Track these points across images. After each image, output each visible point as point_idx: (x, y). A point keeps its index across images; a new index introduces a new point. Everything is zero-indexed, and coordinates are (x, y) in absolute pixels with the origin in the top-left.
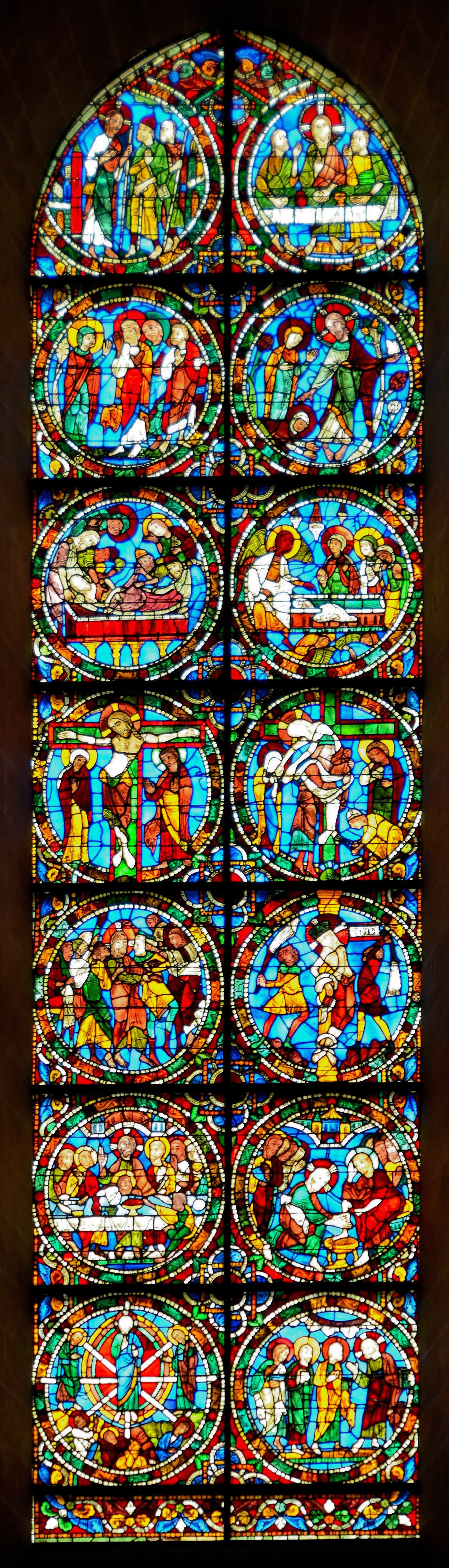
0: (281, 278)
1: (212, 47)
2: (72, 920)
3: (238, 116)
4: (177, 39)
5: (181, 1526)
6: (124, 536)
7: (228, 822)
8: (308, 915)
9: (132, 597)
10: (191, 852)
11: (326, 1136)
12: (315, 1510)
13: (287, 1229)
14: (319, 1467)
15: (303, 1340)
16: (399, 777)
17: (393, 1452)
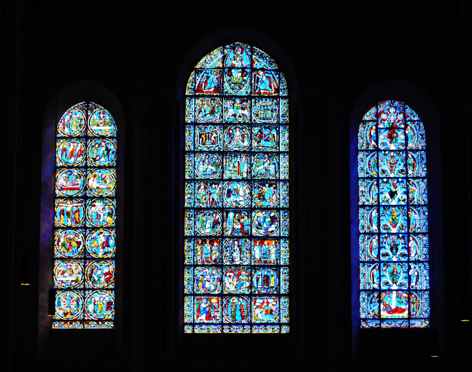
0: (95, 137)
1: (85, 103)
2: (61, 232)
3: (89, 114)
4: (80, 102)
5: (77, 326)
6: (70, 175)
7: (86, 218)
8: (98, 232)
9: (71, 184)
10: (80, 222)
11: (100, 266)
12: (98, 323)
13: (94, 280)
14: (99, 317)
15: (96, 297)
16: (113, 211)
17: (110, 314)
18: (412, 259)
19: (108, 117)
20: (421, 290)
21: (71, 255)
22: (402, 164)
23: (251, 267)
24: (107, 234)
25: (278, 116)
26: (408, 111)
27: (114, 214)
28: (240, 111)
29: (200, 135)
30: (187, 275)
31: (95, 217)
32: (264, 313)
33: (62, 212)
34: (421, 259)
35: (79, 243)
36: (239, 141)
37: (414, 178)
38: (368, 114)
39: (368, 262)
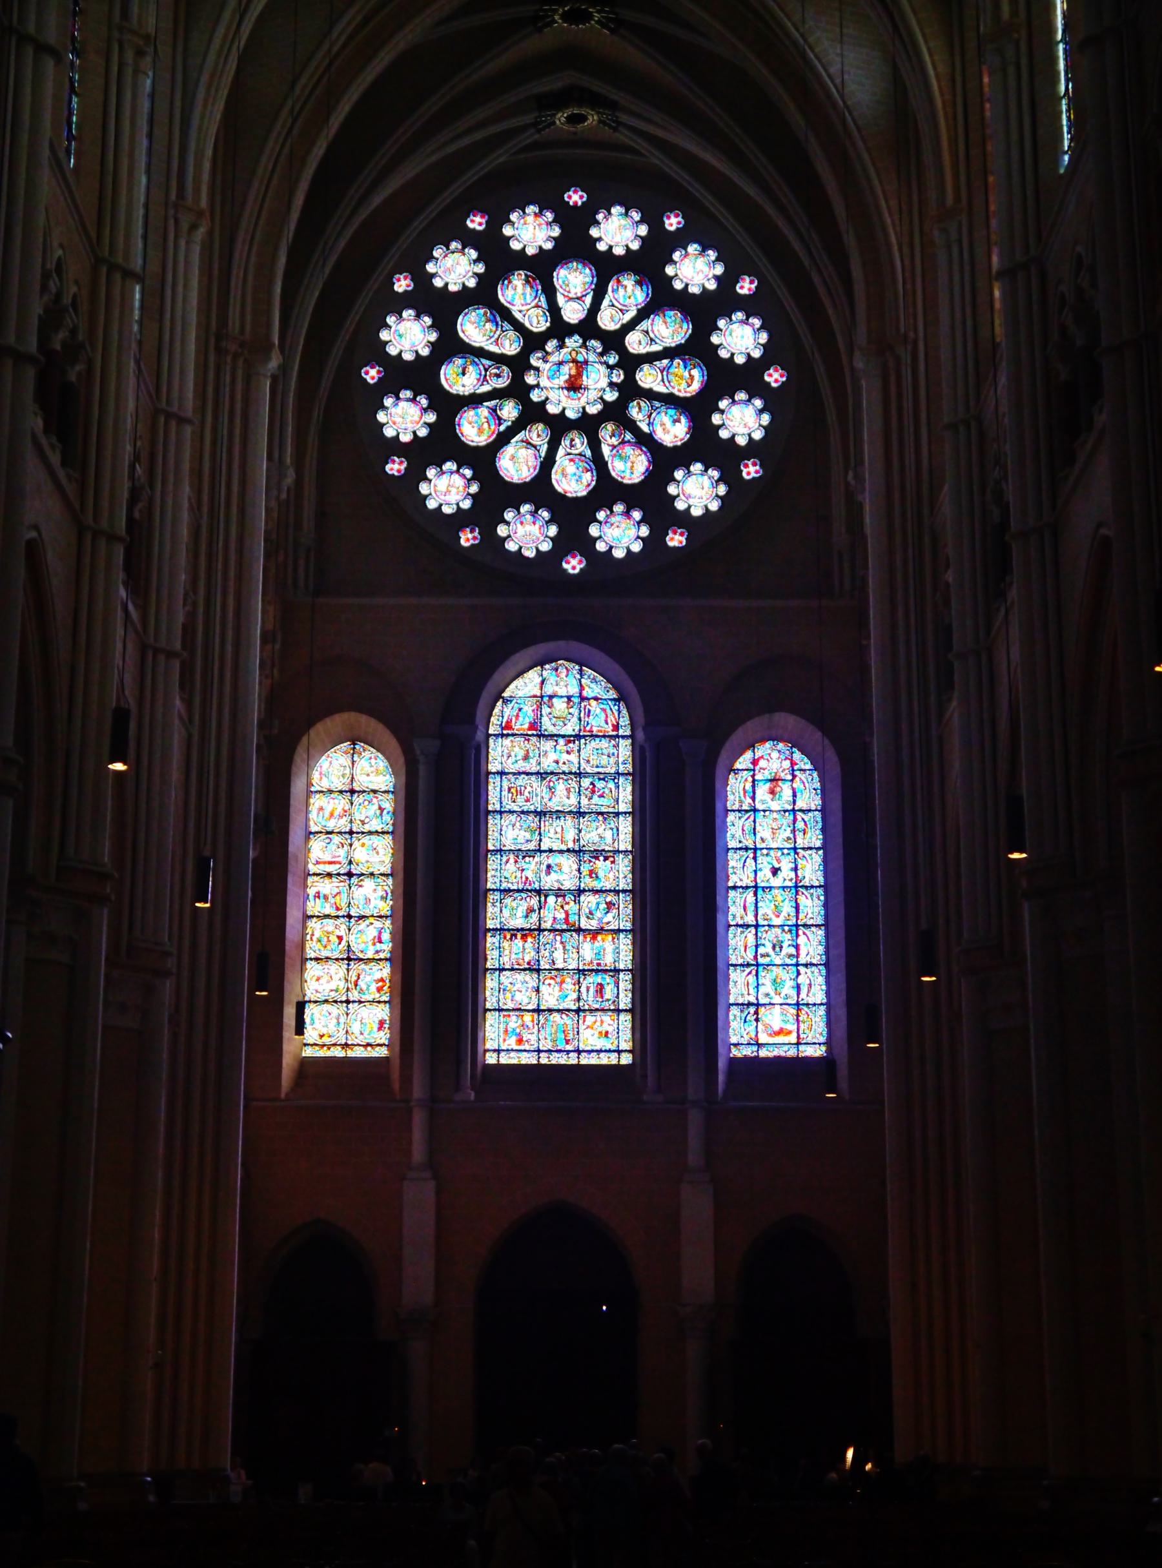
8: (367, 922)
17: (383, 1037)
18: (802, 960)
19: (381, 763)
20: (814, 1005)
21: (329, 954)
22: (789, 830)
23: (581, 972)
24: (378, 924)
25: (617, 763)
26: (797, 756)
27: (389, 897)
28: (565, 757)
29: (509, 789)
30: (491, 982)
31: (362, 902)
32: (597, 1035)
33: (317, 895)
34: (815, 961)
35: (340, 938)
36: (563, 797)
37: (803, 849)
38: (741, 759)
39: (741, 965)
